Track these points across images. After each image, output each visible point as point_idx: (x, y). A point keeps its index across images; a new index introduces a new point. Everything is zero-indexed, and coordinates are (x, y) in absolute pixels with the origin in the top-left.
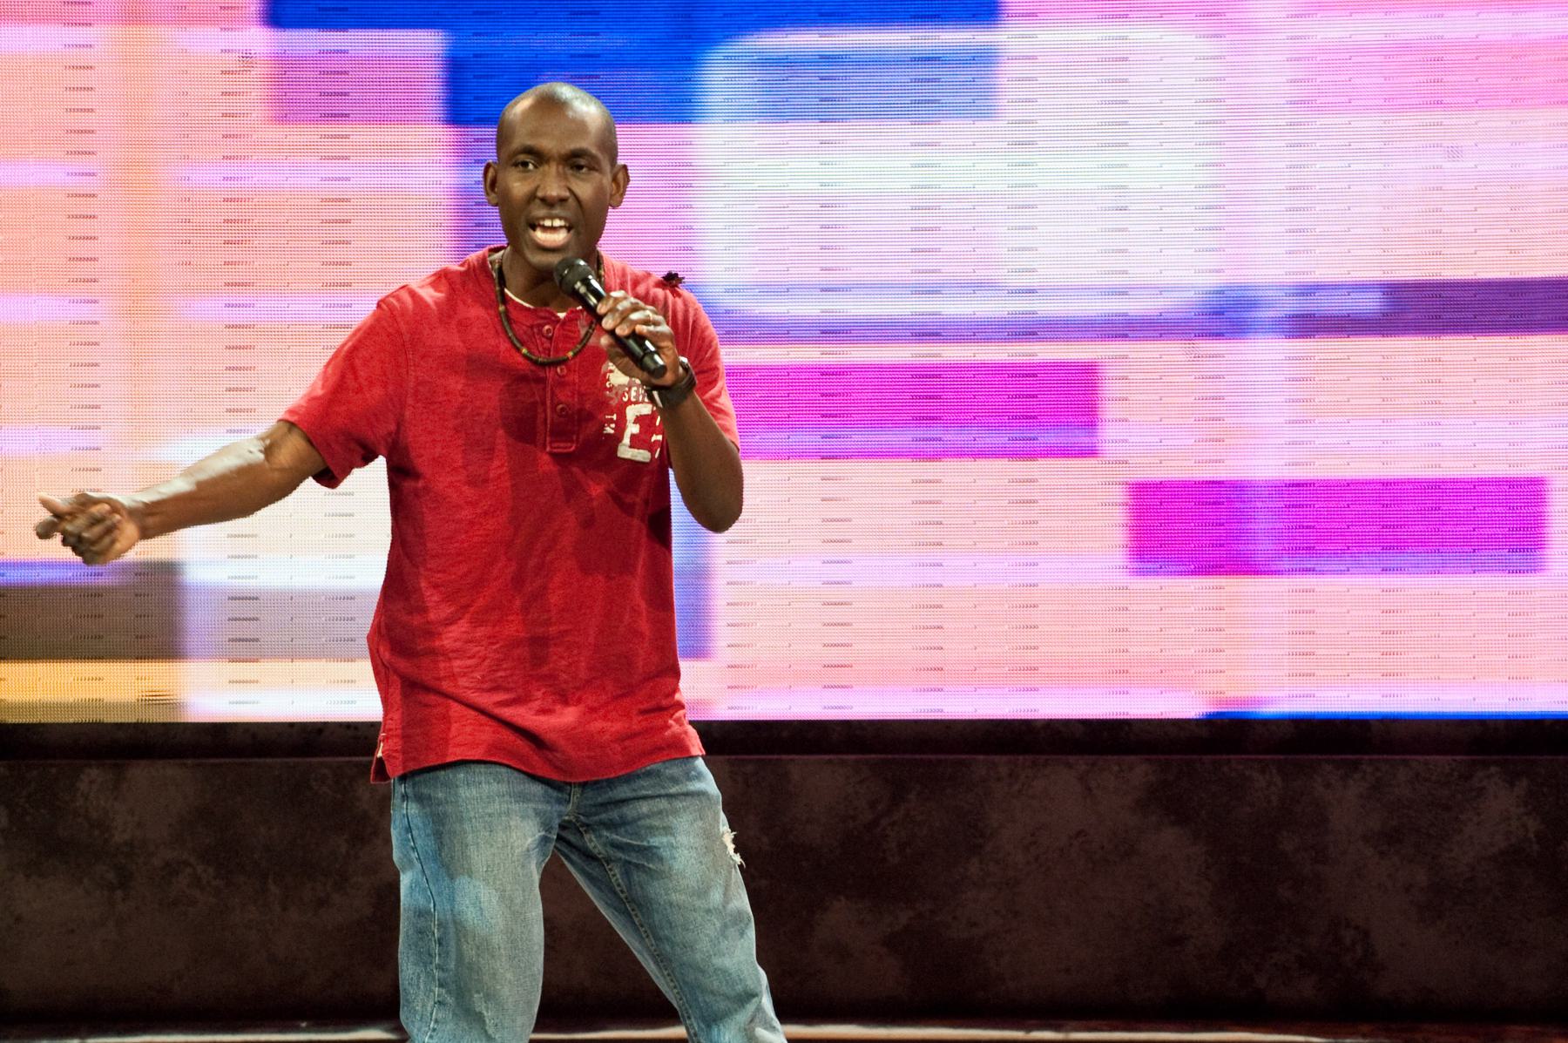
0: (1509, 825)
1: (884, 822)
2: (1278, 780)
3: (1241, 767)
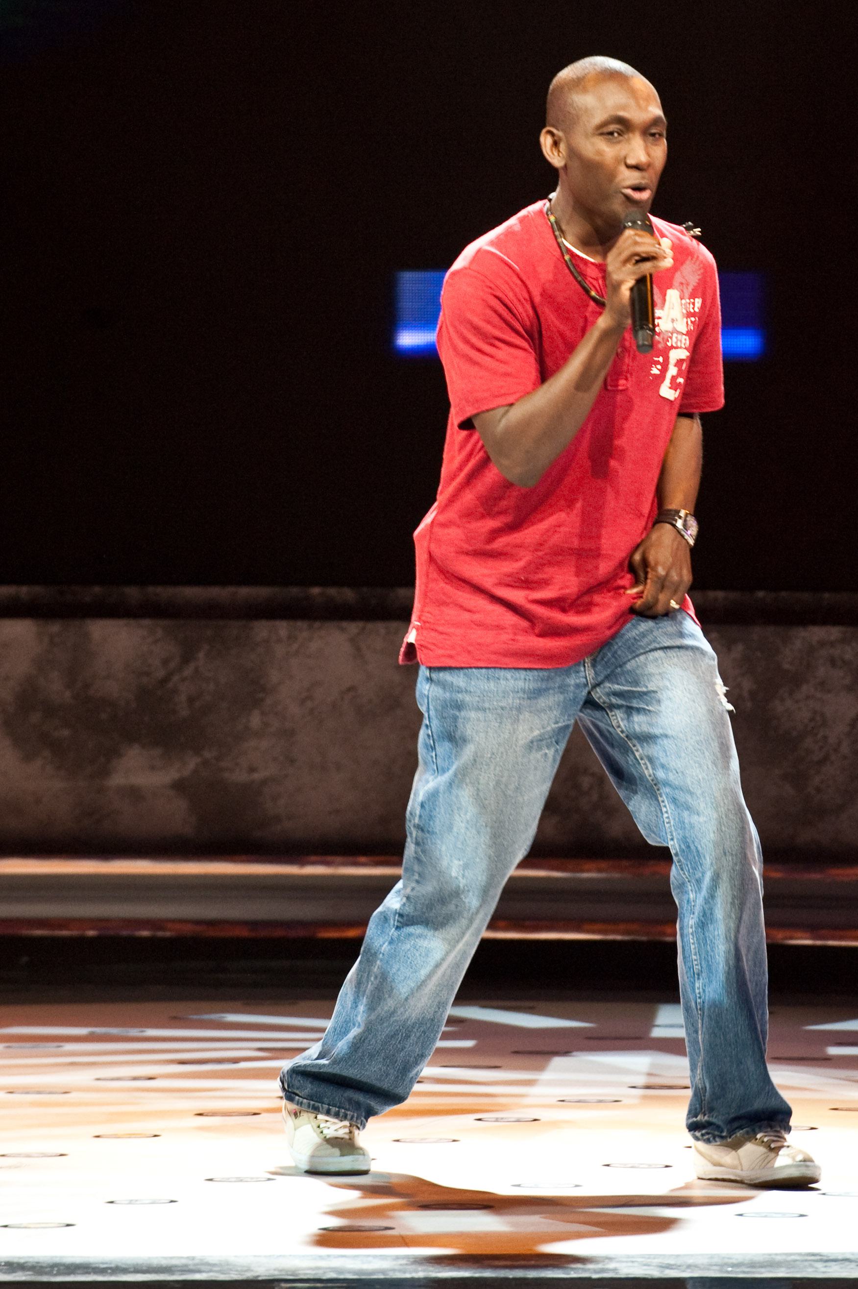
1: (176, 678)
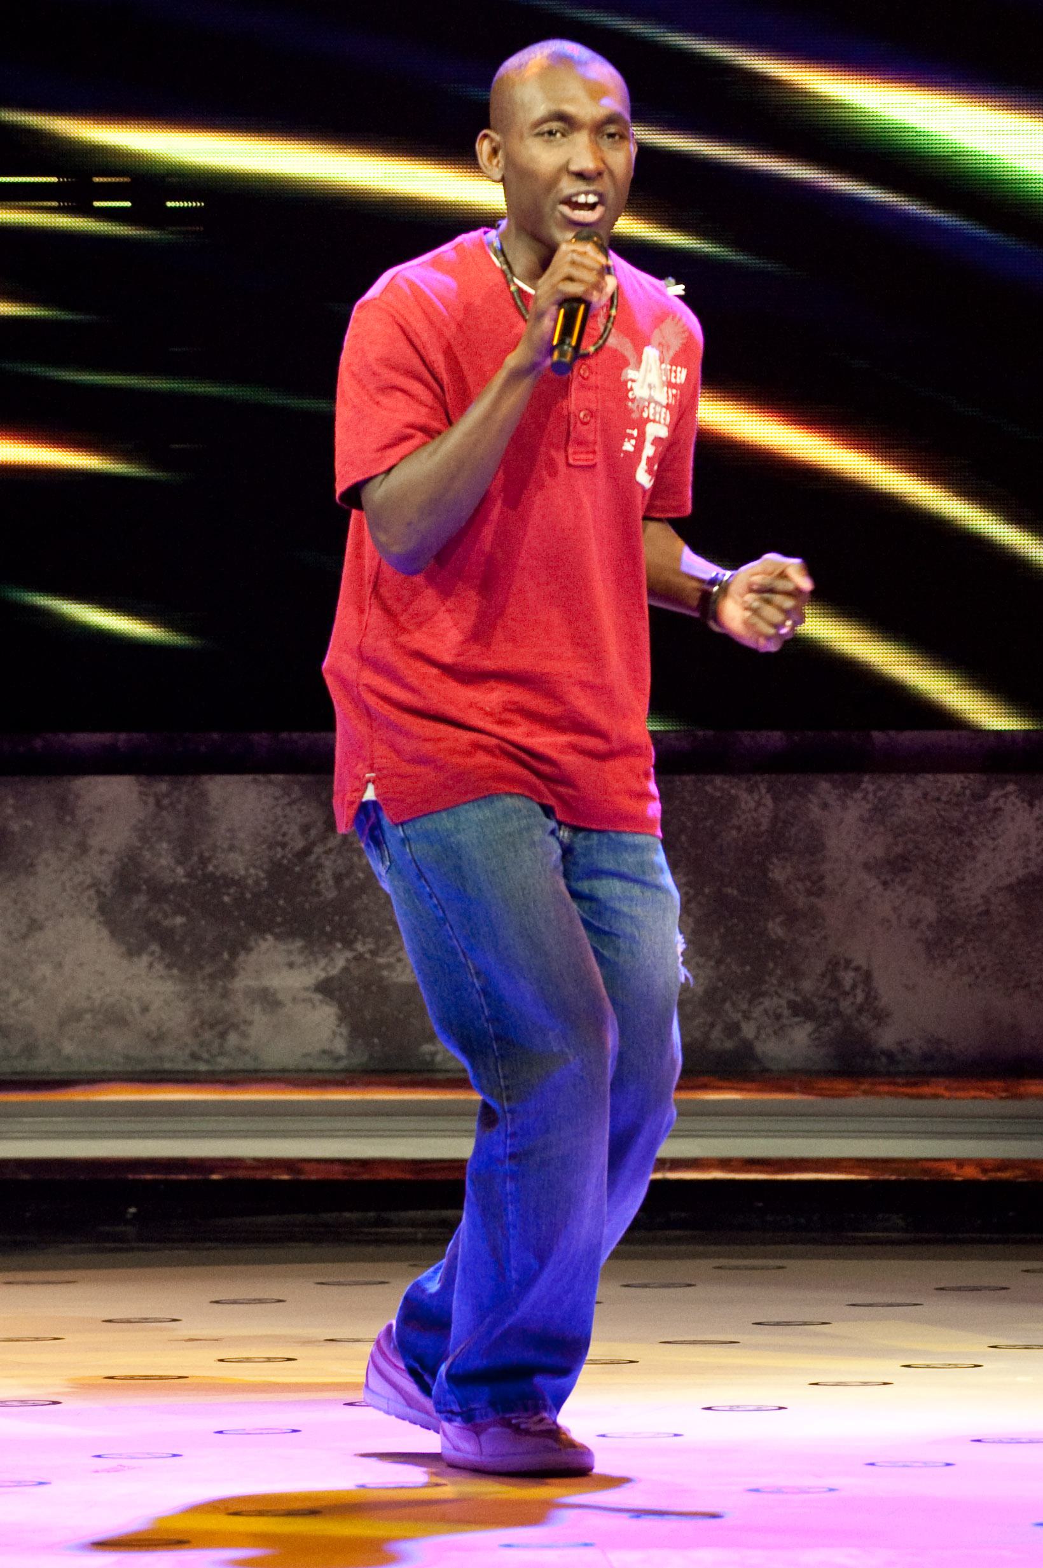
0: (1028, 851)
1: (318, 850)
2: (768, 801)
3: (726, 786)
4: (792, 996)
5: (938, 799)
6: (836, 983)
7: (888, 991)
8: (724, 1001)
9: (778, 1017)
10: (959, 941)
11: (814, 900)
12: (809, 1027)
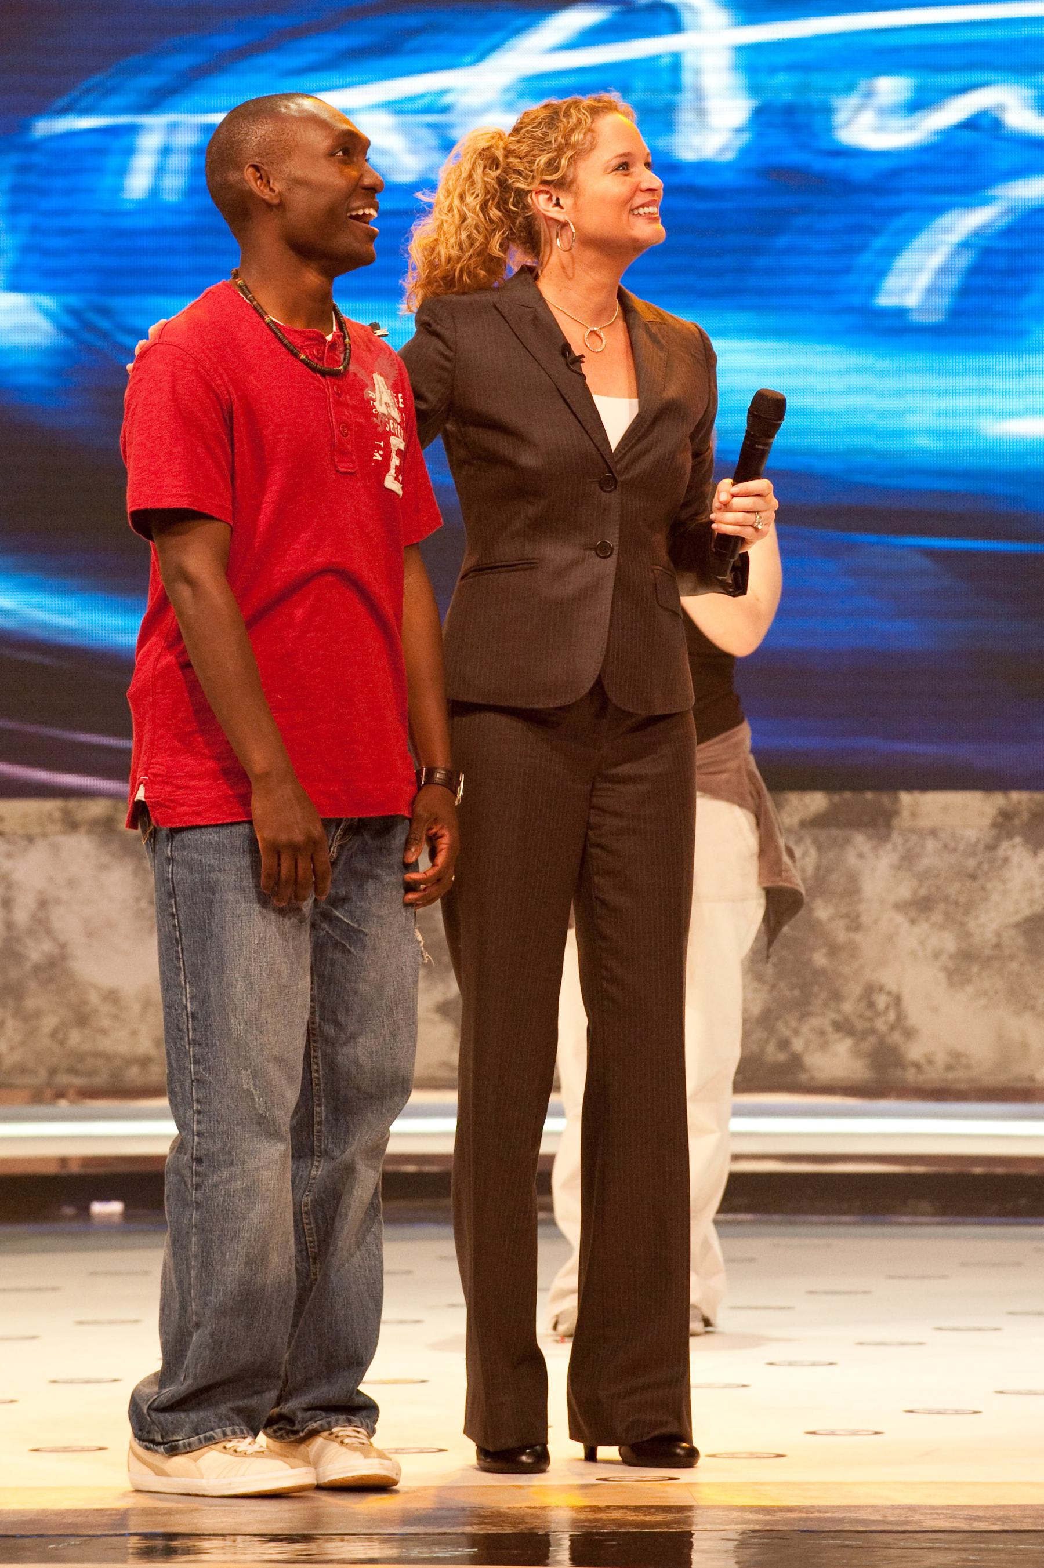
4: (833, 1015)
5: (955, 850)
6: (871, 1005)
7: (915, 1013)
8: (777, 1019)
9: (822, 1033)
10: (975, 969)
11: (852, 935)
12: (848, 1043)
